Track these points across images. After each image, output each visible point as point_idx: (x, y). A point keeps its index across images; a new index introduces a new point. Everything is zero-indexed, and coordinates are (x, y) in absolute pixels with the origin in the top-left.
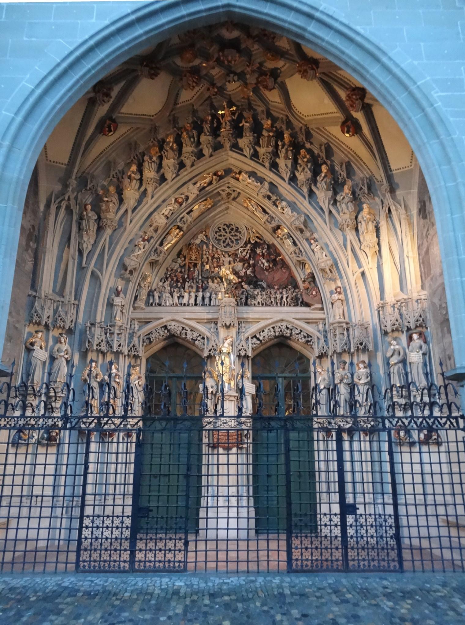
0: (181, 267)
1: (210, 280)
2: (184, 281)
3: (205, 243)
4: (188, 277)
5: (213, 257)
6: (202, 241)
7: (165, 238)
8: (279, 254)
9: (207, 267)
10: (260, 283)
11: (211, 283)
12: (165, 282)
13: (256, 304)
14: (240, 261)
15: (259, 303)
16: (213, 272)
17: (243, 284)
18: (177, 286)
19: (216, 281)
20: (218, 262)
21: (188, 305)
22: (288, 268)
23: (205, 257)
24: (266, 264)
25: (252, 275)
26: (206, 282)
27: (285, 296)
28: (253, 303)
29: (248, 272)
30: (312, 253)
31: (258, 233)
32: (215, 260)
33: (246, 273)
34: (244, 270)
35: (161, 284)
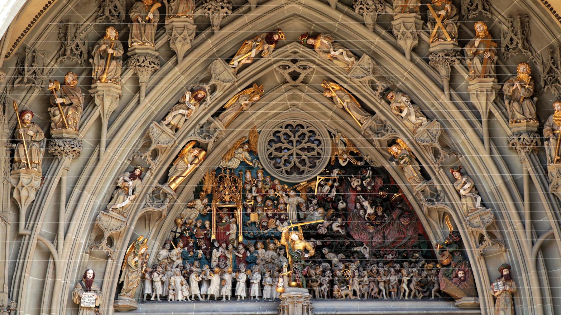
0: (202, 216)
1: (259, 245)
2: (211, 245)
3: (250, 168)
4: (218, 239)
5: (265, 198)
6: (242, 163)
7: (171, 165)
8: (397, 189)
9: (253, 217)
10: (358, 249)
11: (261, 251)
12: (172, 248)
13: (351, 294)
14: (320, 206)
15: (355, 294)
16: (266, 228)
17: (325, 250)
18: (195, 257)
19: (271, 246)
20: (276, 207)
21: (220, 299)
22: (413, 215)
23: (249, 196)
24: (370, 211)
25: (342, 232)
26: (252, 249)
27: (405, 279)
28: (343, 293)
29: (335, 227)
30: (457, 197)
31: (354, 145)
32: (269, 203)
33: (330, 228)
34: (327, 224)
35: (164, 253)
